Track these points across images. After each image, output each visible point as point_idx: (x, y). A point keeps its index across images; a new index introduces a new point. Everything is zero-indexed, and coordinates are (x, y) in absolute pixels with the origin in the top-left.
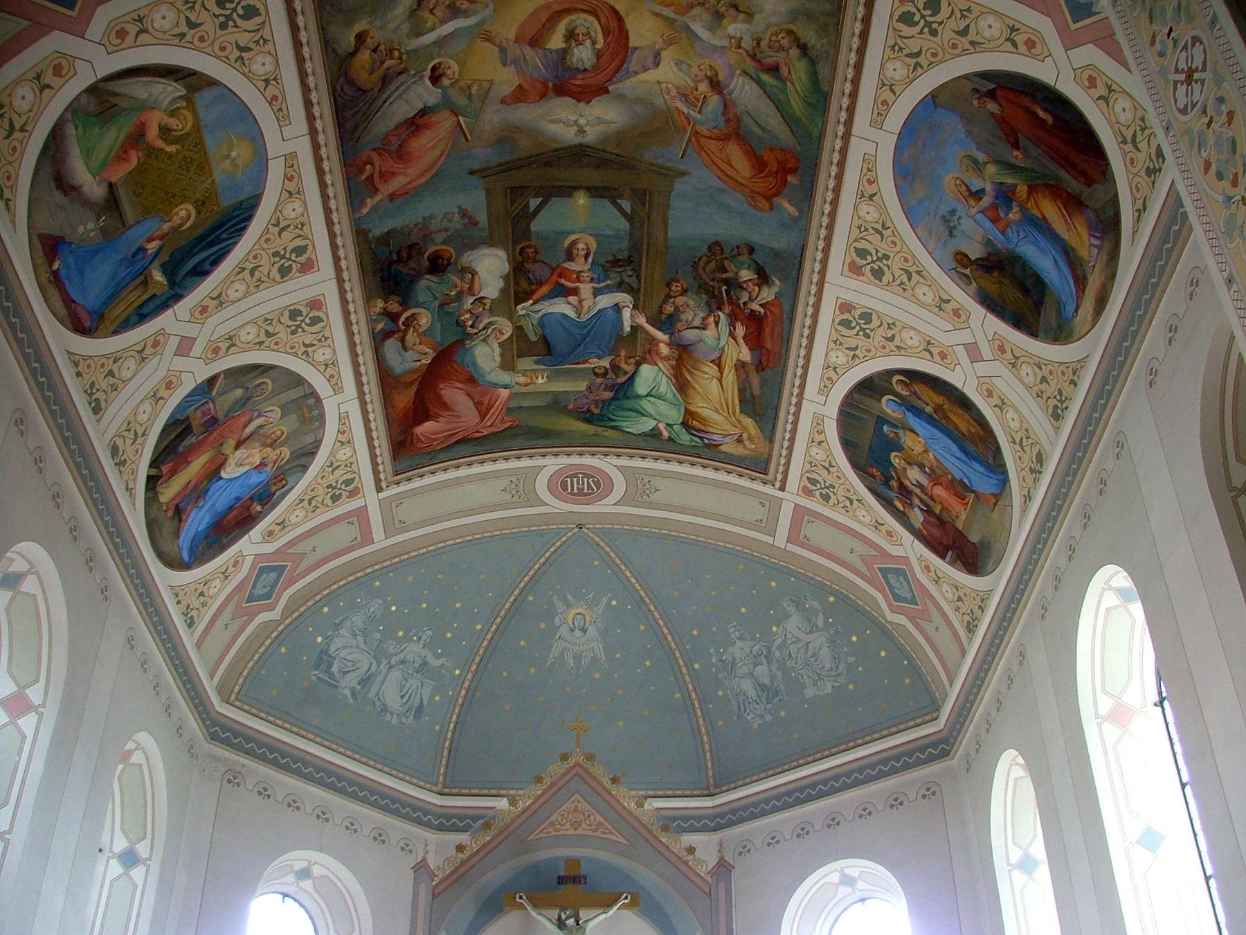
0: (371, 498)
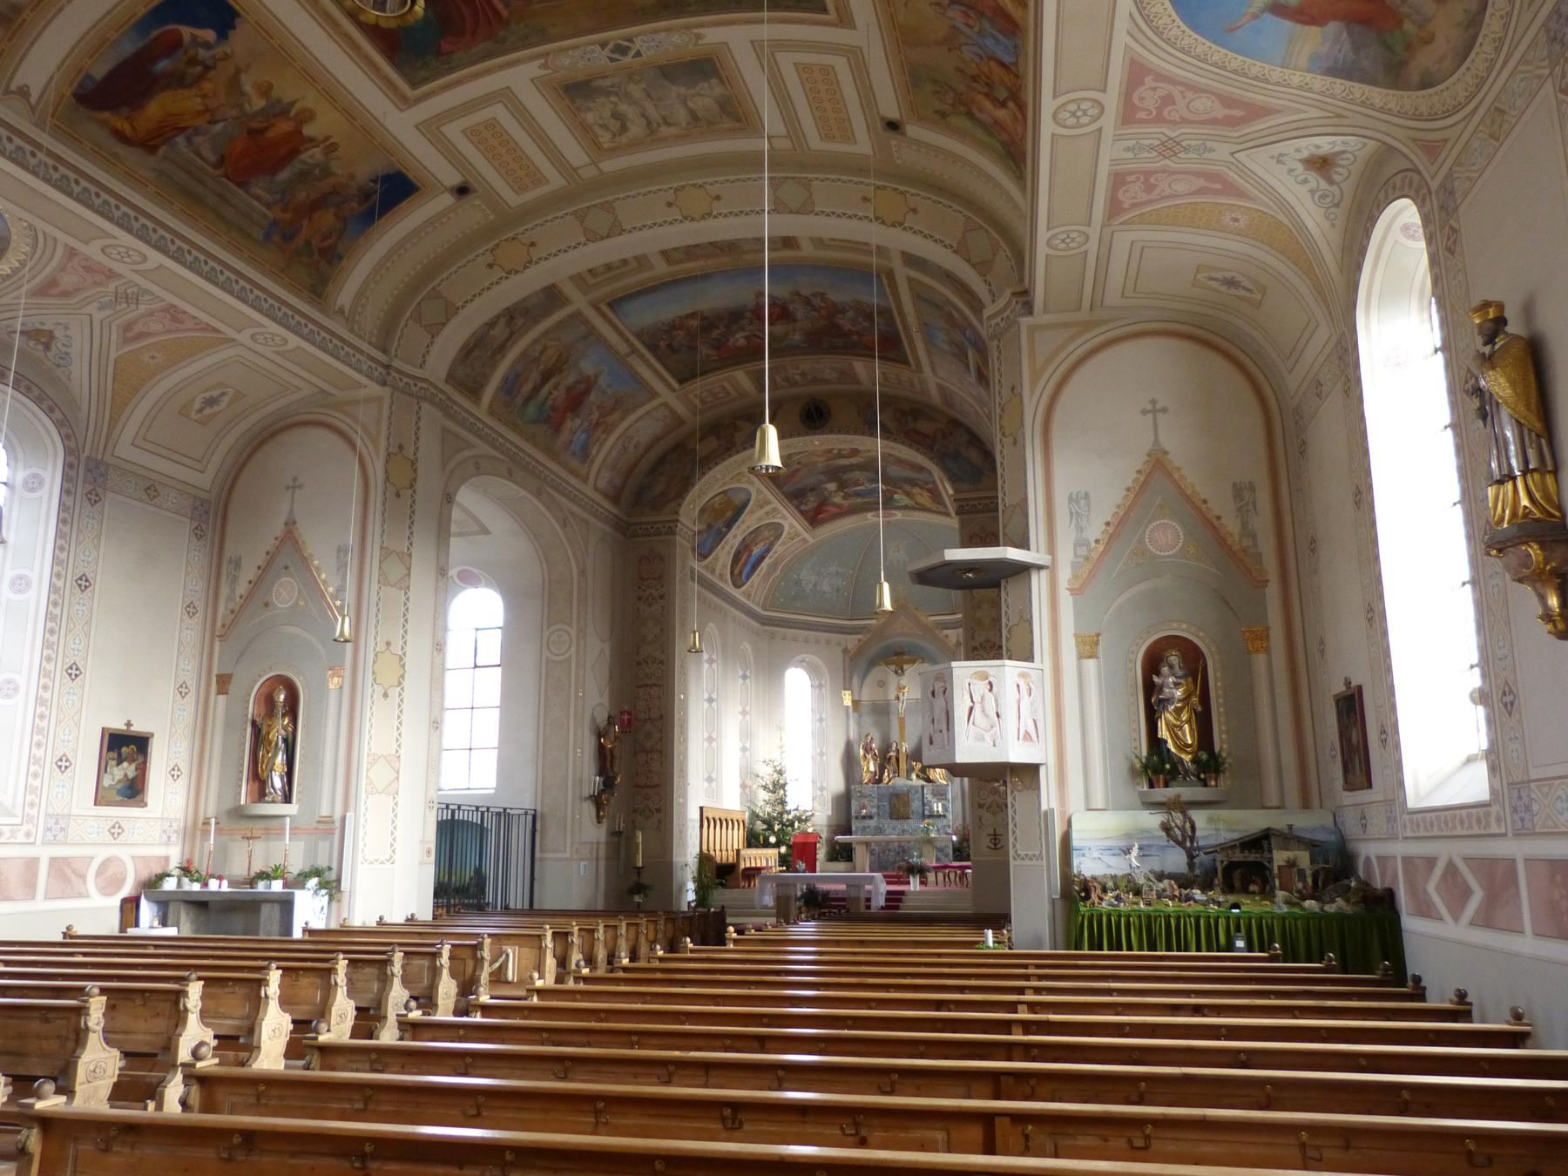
0: (806, 536)
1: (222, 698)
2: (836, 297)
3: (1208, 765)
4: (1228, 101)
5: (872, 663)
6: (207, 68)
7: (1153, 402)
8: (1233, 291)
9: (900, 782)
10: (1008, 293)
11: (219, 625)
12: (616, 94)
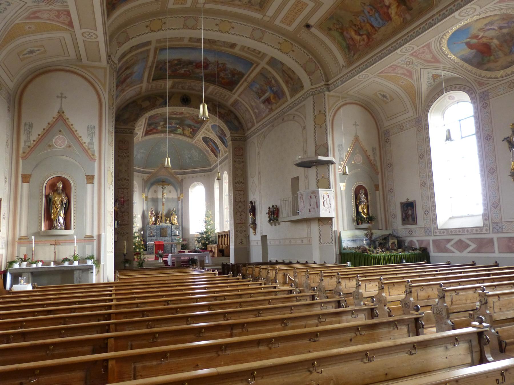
0: (140, 138)
1: (26, 185)
2: (229, 66)
3: (370, 219)
4: (434, 57)
5: (152, 184)
7: (356, 122)
8: (382, 98)
9: (163, 224)
10: (323, 83)
11: (21, 151)
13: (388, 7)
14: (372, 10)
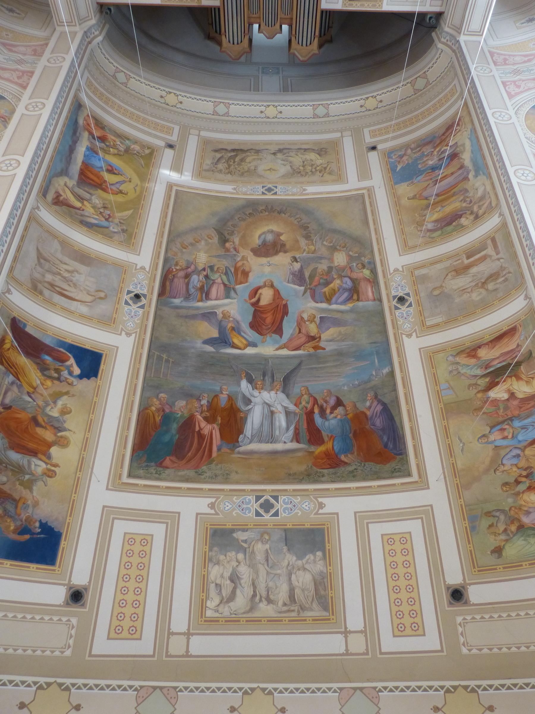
6: (58, 379)
12: (244, 551)
13: (512, 395)
14: (503, 430)
